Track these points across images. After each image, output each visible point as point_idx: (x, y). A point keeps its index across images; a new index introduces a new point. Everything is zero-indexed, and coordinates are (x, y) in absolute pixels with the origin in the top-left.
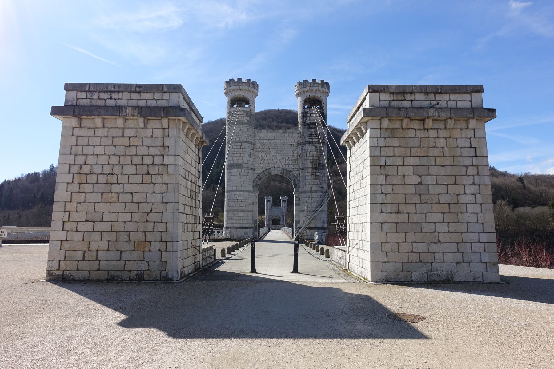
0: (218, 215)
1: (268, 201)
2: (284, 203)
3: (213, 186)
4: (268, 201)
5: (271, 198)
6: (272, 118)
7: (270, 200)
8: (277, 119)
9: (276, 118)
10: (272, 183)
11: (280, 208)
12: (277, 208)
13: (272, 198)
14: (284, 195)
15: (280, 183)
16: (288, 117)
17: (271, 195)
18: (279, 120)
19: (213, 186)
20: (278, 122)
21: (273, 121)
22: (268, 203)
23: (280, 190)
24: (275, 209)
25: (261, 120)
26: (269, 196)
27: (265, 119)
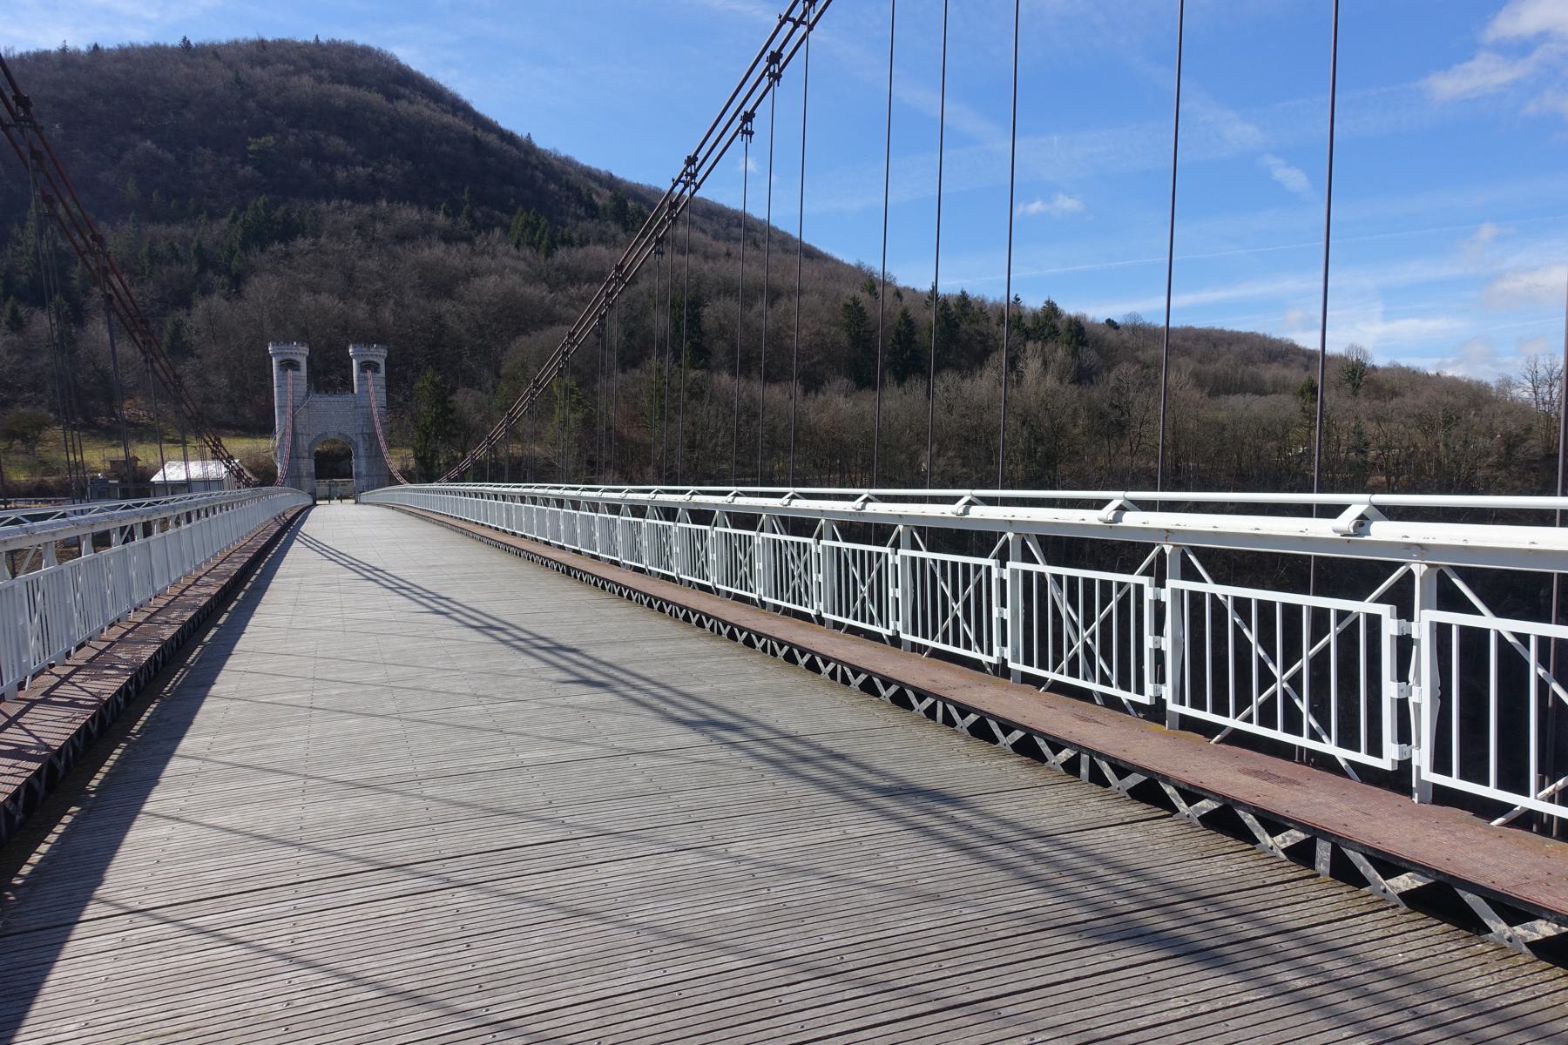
0: (37, 440)
1: (287, 365)
2: (369, 374)
3: (14, 312)
4: (287, 365)
5: (301, 353)
6: (293, 63)
7: (298, 358)
8: (314, 67)
9: (307, 64)
10: (306, 299)
11: (349, 397)
12: (336, 398)
13: (305, 350)
14: (366, 340)
15: (342, 298)
16: (361, 65)
17: (303, 336)
18: (324, 73)
19: (14, 312)
20: (320, 80)
21: (299, 72)
22: (290, 371)
23: (345, 329)
24: (322, 402)
25: (246, 67)
26: (288, 341)
27: (264, 63)
